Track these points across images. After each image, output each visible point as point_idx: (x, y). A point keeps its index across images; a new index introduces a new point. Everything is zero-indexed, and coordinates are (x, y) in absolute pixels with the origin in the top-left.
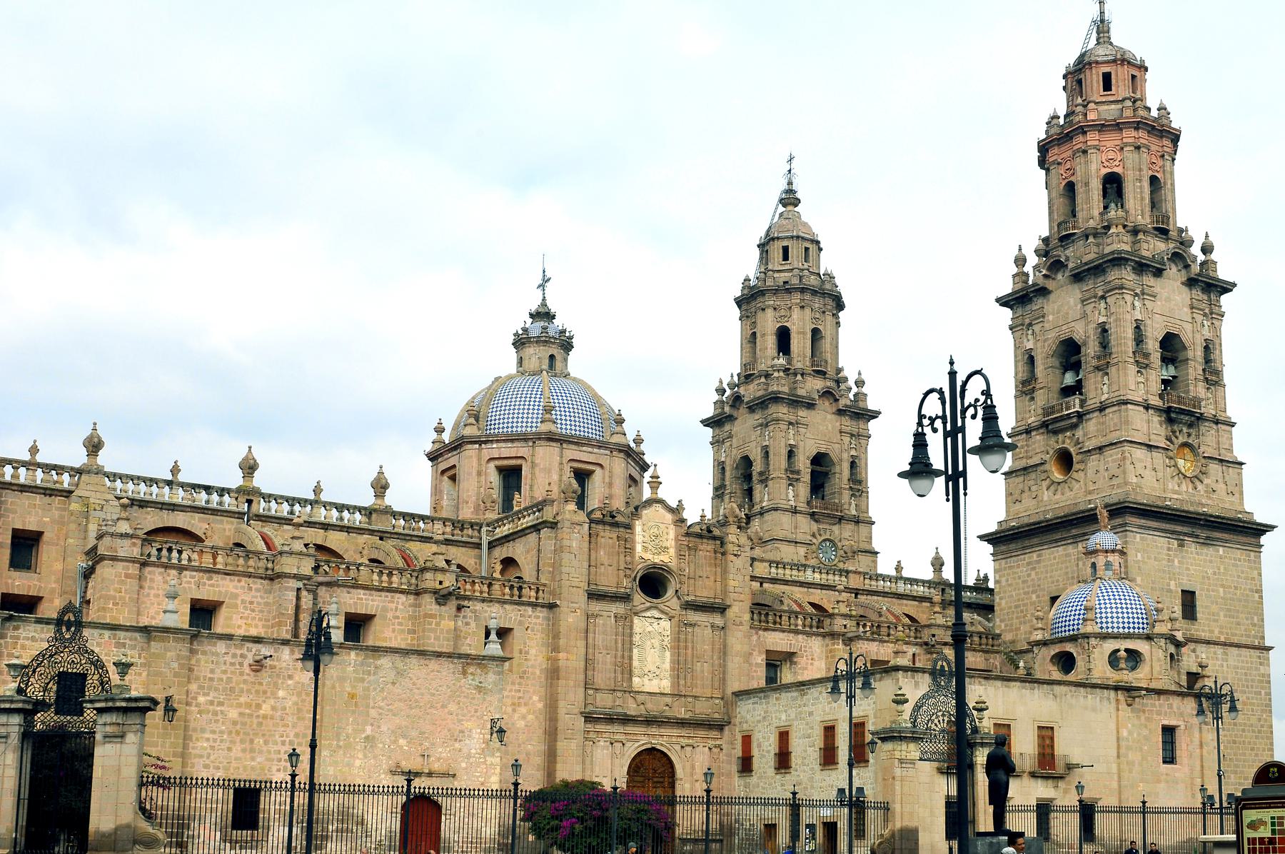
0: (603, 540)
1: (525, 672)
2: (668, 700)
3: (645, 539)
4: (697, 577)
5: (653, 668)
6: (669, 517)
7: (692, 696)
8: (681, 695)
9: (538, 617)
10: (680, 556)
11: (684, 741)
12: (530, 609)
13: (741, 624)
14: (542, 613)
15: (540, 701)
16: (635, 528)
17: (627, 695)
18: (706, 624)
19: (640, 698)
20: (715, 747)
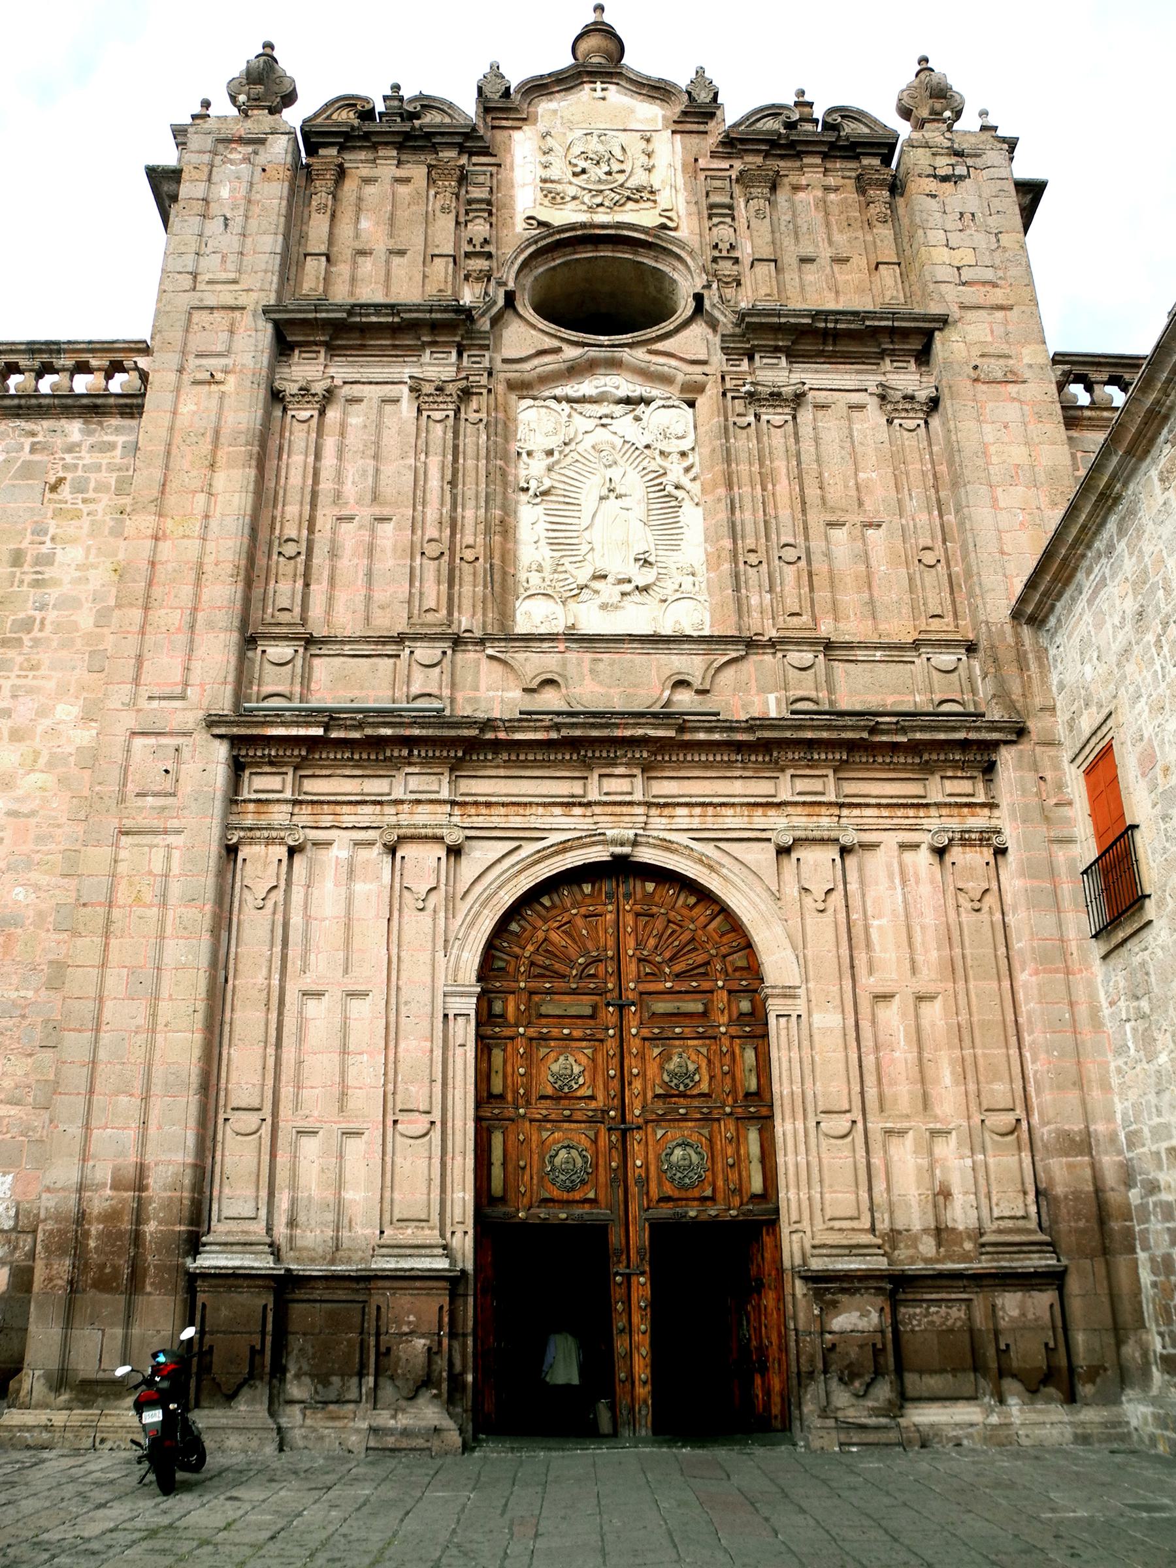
2: (692, 665)
4: (789, 258)
5: (620, 565)
6: (651, 113)
7: (812, 643)
8: (751, 644)
11: (780, 825)
12: (74, 429)
13: (1012, 378)
16: (508, 150)
20: (965, 842)
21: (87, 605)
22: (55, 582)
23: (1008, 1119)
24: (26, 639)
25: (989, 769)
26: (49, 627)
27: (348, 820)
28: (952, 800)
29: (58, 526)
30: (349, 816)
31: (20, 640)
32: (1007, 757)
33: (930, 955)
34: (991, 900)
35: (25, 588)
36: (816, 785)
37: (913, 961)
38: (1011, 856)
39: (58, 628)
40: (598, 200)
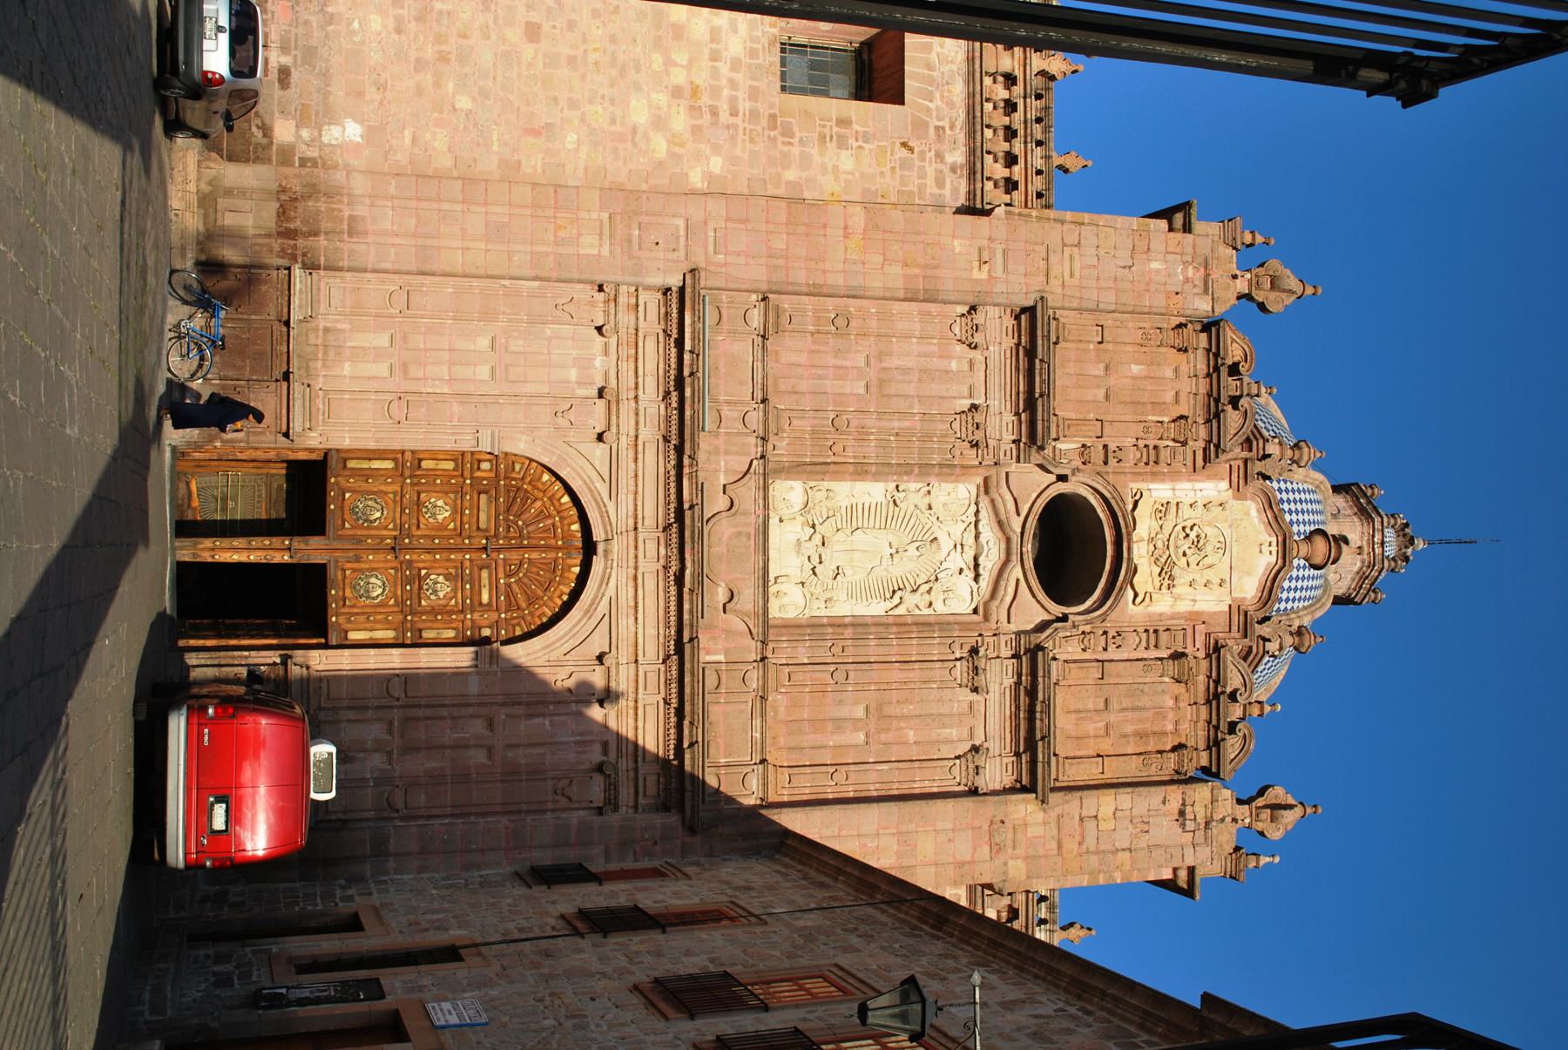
0: (1169, 373)
1: (788, 133)
3: (1186, 512)
7: (764, 687)
9: (940, 183)
10: (1153, 633)
12: (958, 156)
14: (956, 191)
15: (710, 177)
16: (1209, 478)
17: (753, 447)
18: (980, 733)
19: (747, 493)
20: (612, 787)
21: (804, 175)
22: (822, 153)
23: (400, 804)
24: (776, 132)
25: (666, 808)
26: (785, 148)
27: (623, 366)
28: (641, 779)
29: (871, 150)
30: (627, 368)
31: (774, 128)
32: (673, 819)
33: (521, 757)
34: (564, 802)
35: (818, 129)
36: (652, 687)
37: (518, 746)
38: (597, 820)
39: (785, 155)
40: (1160, 544)
